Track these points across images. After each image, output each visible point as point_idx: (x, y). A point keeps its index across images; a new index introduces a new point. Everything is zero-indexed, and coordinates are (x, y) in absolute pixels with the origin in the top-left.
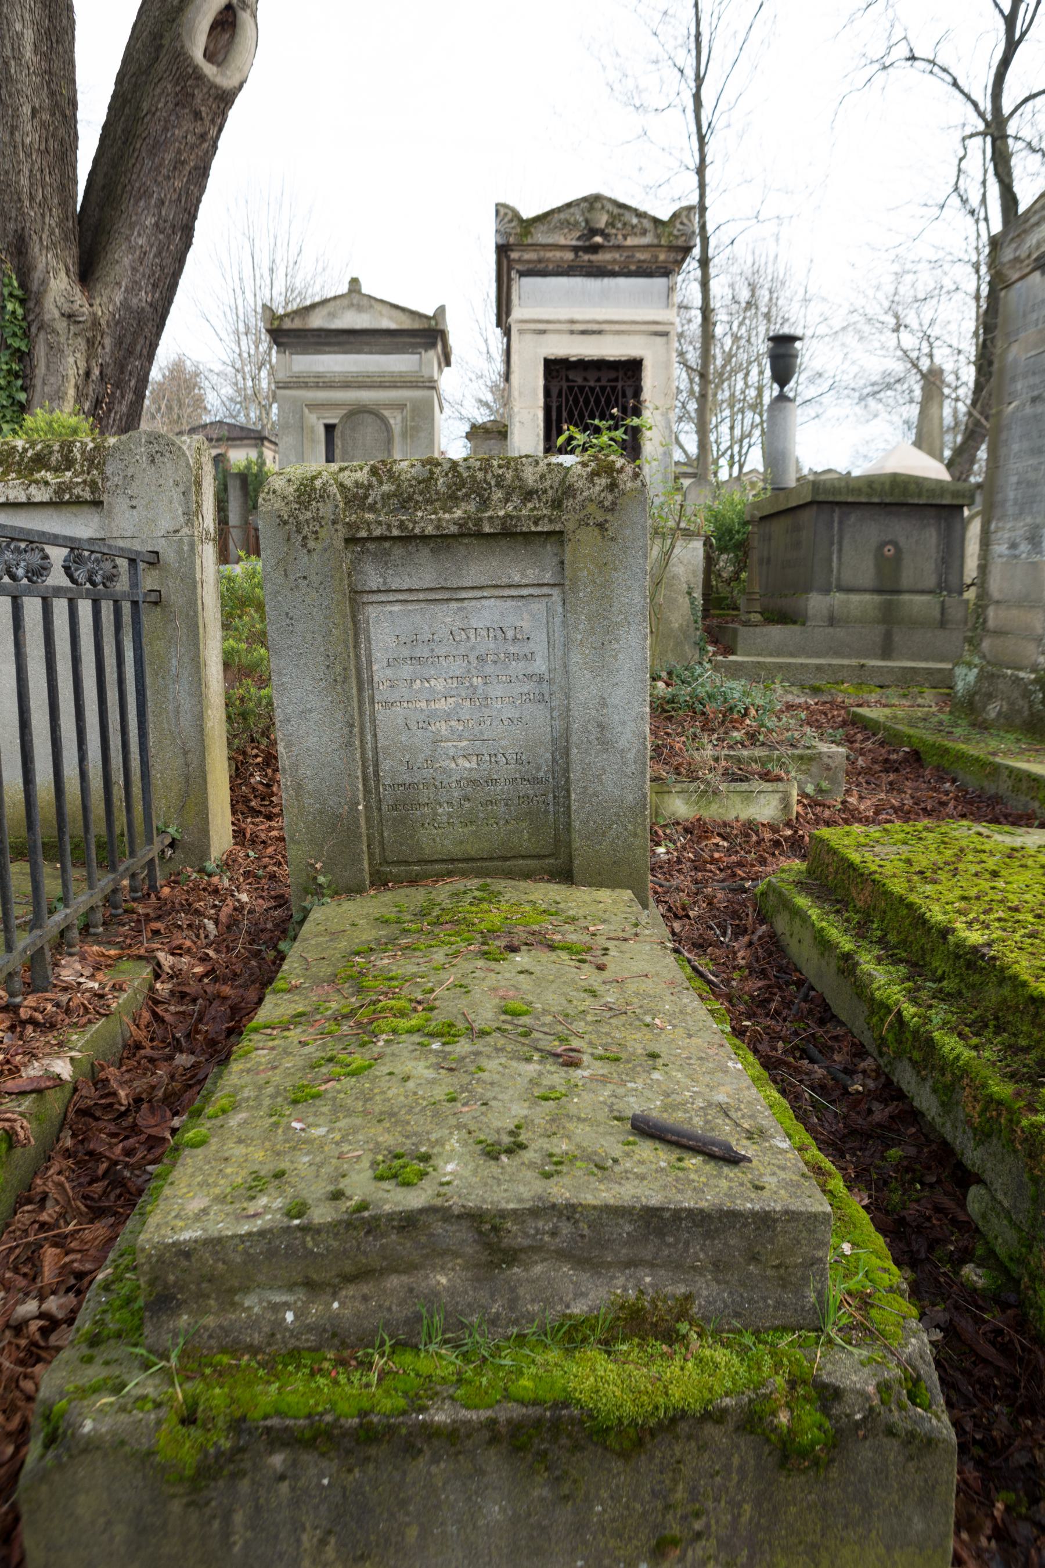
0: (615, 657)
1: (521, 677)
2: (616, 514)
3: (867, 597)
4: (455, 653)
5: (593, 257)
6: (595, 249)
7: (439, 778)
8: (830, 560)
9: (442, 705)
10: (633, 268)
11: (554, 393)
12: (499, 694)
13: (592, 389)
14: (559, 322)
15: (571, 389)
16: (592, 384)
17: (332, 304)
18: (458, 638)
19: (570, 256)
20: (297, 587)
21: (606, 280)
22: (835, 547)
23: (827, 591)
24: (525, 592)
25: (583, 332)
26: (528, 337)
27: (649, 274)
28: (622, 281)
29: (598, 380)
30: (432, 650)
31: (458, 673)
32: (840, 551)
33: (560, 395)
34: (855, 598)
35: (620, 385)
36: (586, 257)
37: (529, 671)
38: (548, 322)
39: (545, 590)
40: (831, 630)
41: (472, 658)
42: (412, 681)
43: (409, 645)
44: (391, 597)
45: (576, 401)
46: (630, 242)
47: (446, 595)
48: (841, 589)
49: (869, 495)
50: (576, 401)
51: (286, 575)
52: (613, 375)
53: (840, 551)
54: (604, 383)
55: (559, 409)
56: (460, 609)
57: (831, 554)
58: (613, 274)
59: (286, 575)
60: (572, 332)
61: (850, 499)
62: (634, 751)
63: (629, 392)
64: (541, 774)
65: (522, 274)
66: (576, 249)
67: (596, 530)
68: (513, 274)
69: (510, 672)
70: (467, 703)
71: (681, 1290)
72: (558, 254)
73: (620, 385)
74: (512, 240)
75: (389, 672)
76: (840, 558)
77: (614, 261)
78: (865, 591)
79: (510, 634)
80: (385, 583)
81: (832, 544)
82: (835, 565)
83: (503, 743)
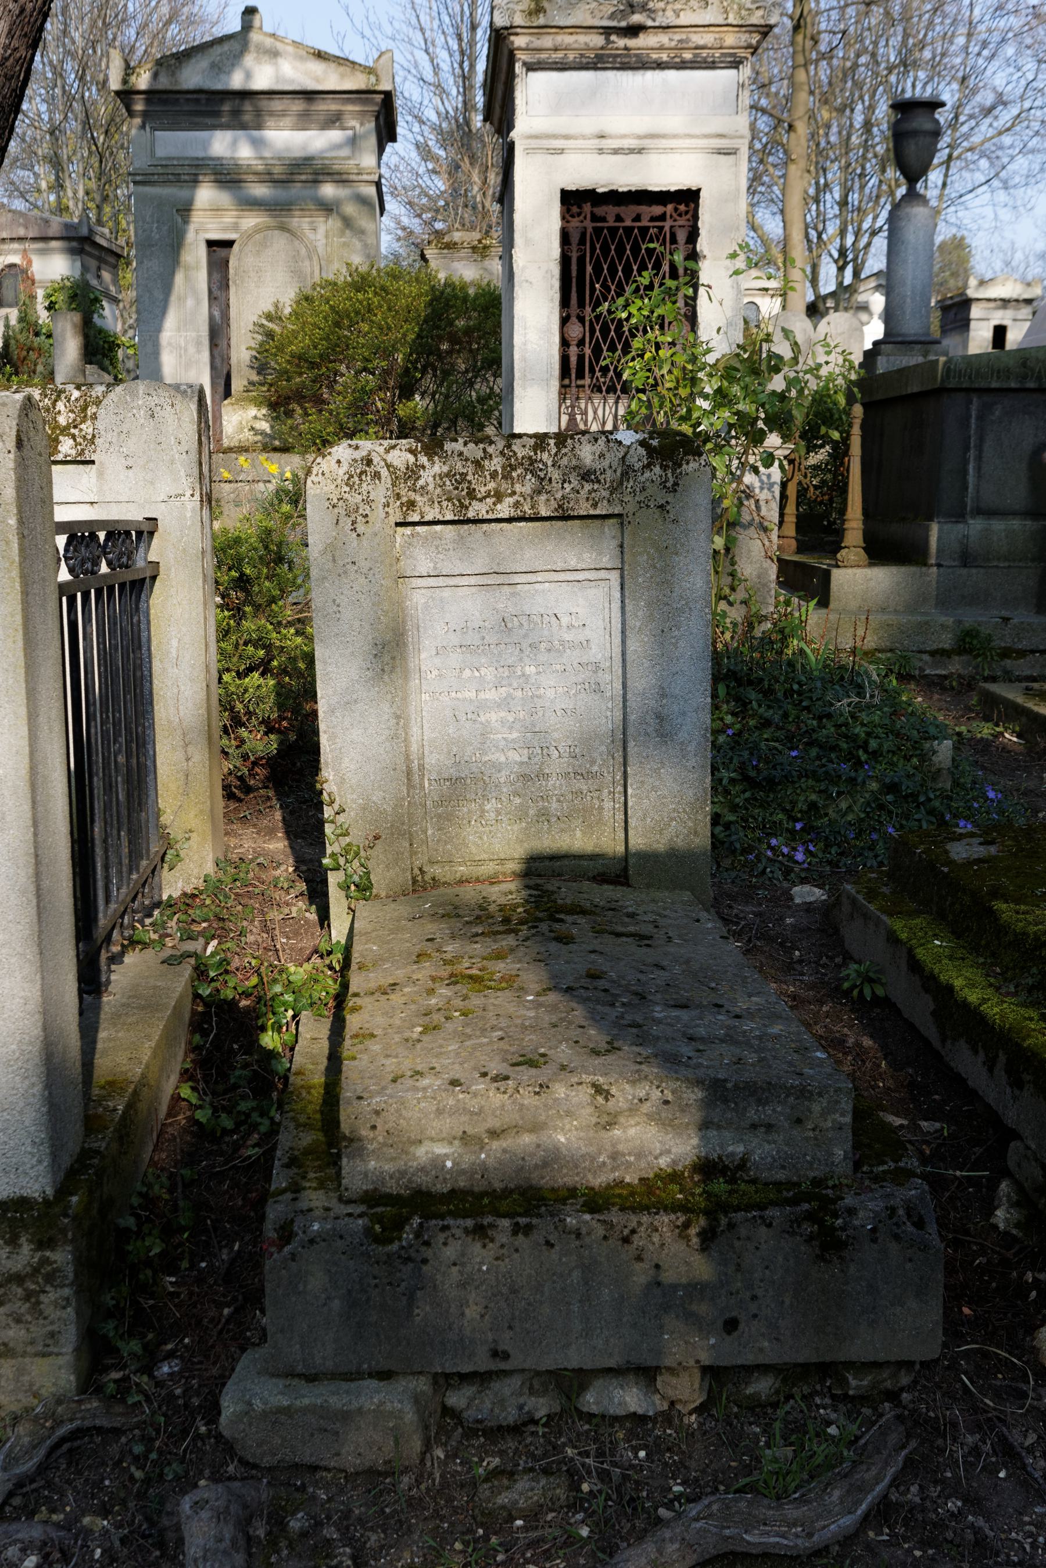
0: (675, 645)
1: (575, 665)
2: (678, 495)
3: (1016, 523)
4: (507, 640)
5: (631, 43)
6: (634, 31)
7: (488, 773)
8: (965, 472)
9: (491, 695)
10: (688, 56)
11: (575, 239)
12: (552, 683)
13: (628, 230)
14: (584, 137)
15: (598, 231)
16: (628, 223)
17: (218, 50)
18: (510, 625)
19: (598, 40)
20: (345, 572)
21: (649, 75)
22: (972, 454)
23: (959, 515)
24: (580, 576)
25: (616, 152)
26: (540, 158)
27: (711, 65)
28: (671, 75)
29: (638, 218)
30: (483, 638)
31: (510, 662)
32: (979, 458)
33: (582, 241)
34: (998, 525)
35: (667, 225)
36: (621, 42)
37: (584, 660)
38: (567, 137)
39: (603, 574)
40: (964, 571)
41: (525, 645)
42: (461, 670)
43: (458, 633)
44: (441, 582)
45: (605, 250)
46: (685, 19)
47: (500, 579)
48: (980, 511)
49: (1024, 377)
50: (605, 250)
51: (334, 561)
52: (657, 210)
53: (979, 458)
54: (645, 223)
55: (581, 261)
56: (513, 594)
57: (966, 462)
58: (660, 66)
59: (334, 561)
60: (601, 151)
61: (994, 385)
62: (694, 743)
63: (682, 236)
64: (595, 768)
65: (530, 68)
66: (607, 31)
67: (657, 511)
68: (518, 68)
69: (564, 661)
70: (519, 694)
71: (740, 1149)
72: (583, 39)
73: (667, 225)
74: (519, 20)
75: (437, 661)
76: (978, 469)
77: (662, 48)
78: (1014, 514)
79: (565, 620)
80: (435, 568)
81: (967, 448)
82: (971, 479)
83: (556, 735)
